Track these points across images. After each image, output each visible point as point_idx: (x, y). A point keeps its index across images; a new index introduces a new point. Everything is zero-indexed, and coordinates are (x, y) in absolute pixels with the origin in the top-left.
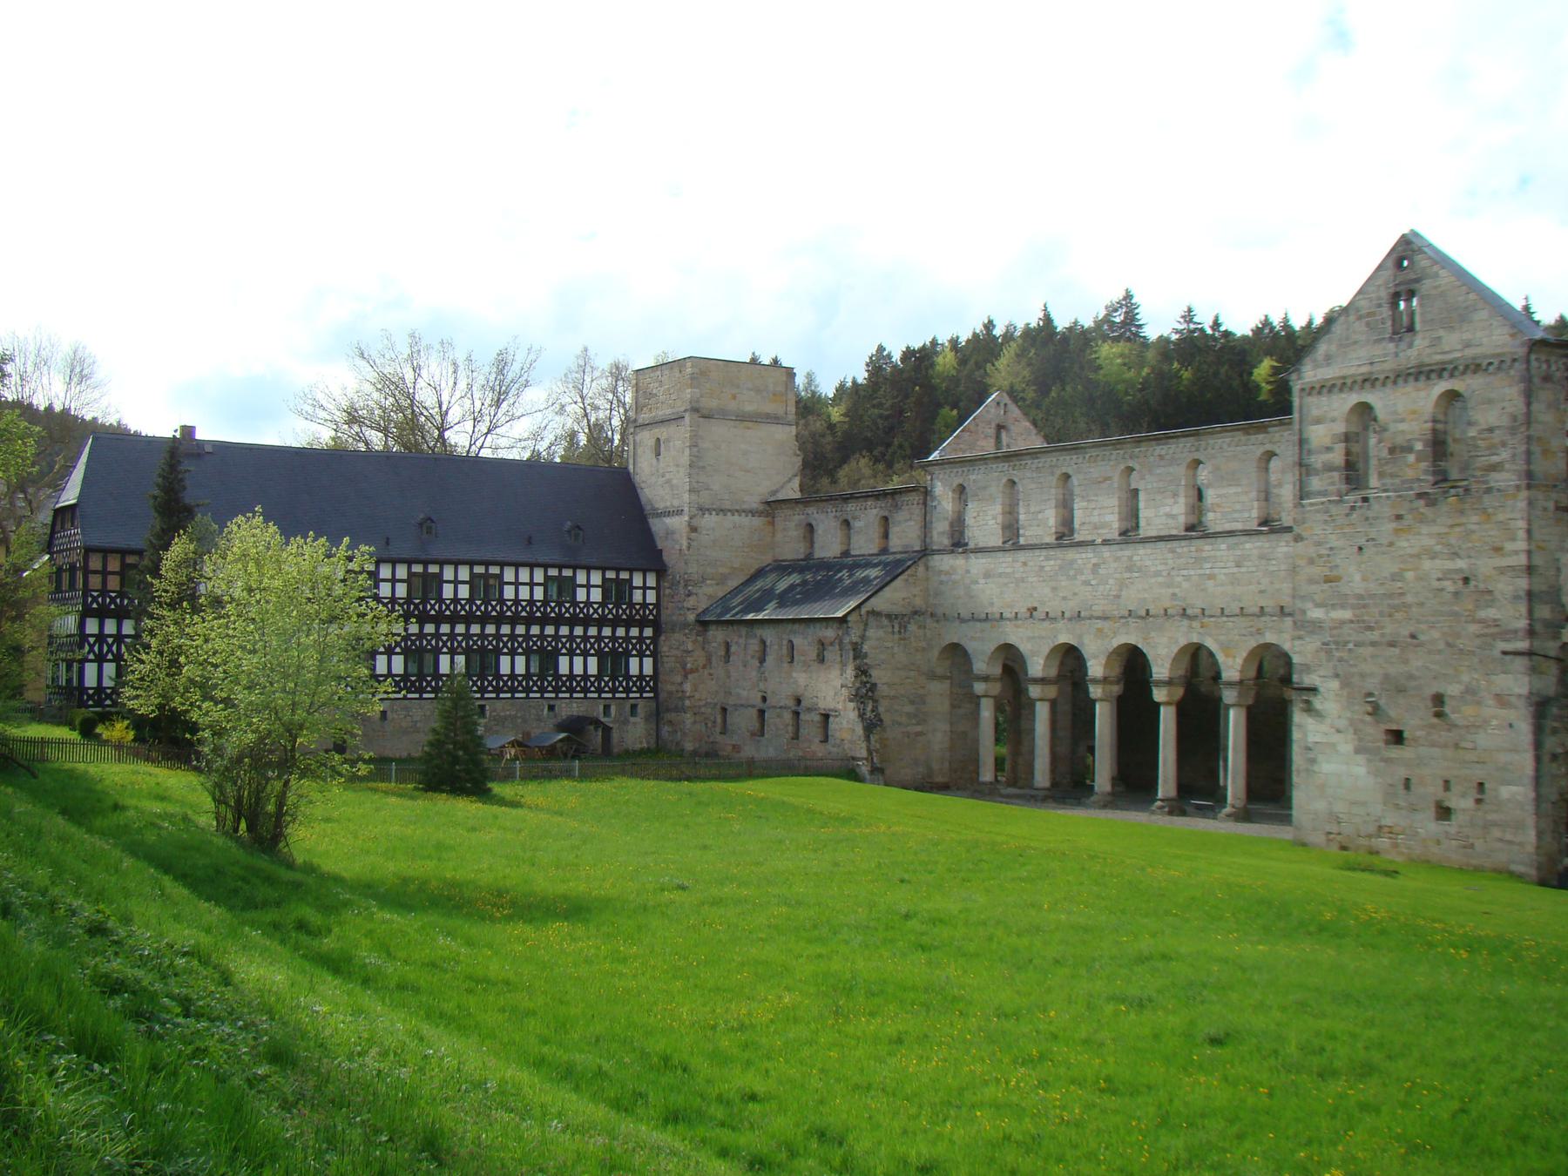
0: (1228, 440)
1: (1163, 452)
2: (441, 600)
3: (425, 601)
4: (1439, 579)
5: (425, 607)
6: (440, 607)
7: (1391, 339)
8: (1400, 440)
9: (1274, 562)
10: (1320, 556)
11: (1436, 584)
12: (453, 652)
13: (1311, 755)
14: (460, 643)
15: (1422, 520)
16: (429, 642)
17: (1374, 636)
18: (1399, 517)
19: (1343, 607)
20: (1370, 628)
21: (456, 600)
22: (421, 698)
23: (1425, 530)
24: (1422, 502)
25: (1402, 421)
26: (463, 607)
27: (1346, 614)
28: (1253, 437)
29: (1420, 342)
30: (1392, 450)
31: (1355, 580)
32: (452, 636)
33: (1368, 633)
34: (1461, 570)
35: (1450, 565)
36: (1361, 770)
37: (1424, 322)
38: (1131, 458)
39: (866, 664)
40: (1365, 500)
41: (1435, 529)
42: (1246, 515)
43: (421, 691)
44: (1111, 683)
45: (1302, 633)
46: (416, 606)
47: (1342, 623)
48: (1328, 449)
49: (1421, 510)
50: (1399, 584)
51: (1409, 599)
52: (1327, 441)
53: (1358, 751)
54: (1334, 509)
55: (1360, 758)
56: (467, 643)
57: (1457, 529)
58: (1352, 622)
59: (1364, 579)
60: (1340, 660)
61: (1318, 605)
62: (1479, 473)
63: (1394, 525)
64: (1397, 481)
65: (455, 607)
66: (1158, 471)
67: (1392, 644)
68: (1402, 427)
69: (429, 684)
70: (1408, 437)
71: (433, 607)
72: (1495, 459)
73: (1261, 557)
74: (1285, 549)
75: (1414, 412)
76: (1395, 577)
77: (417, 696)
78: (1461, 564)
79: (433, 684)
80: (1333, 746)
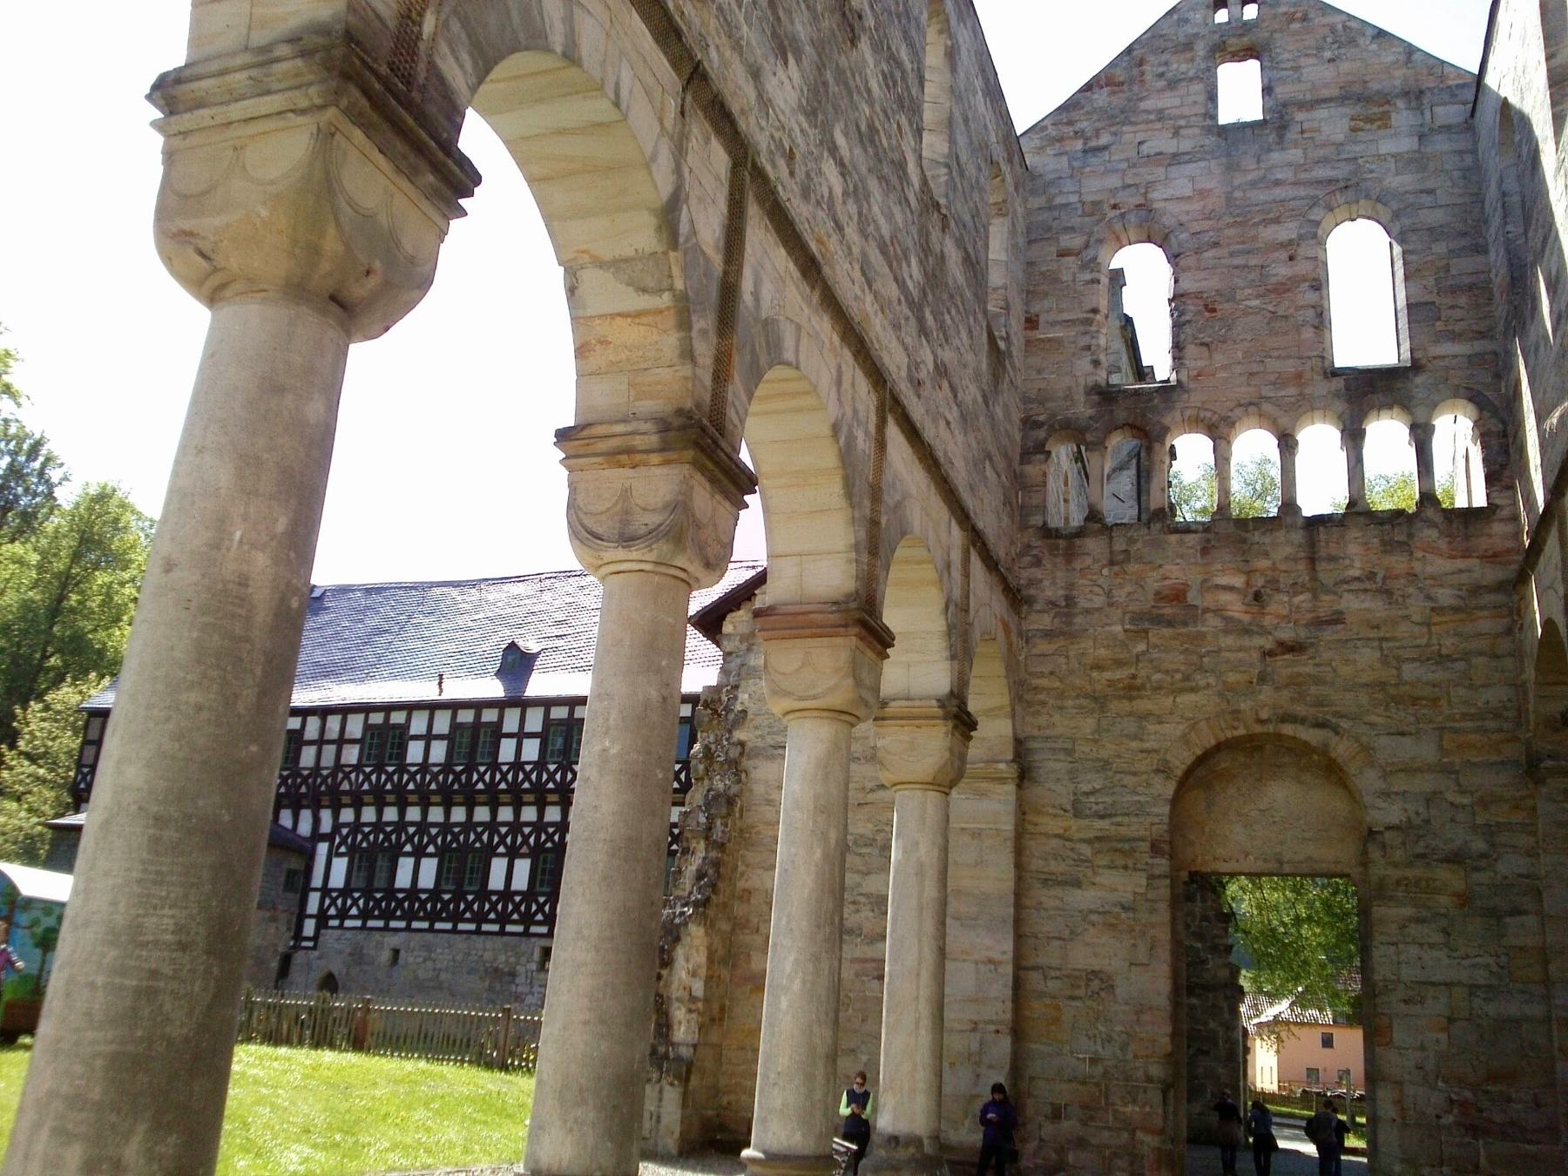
2: (495, 766)
3: (469, 770)
5: (470, 777)
6: (493, 777)
12: (513, 854)
14: (526, 838)
16: (479, 837)
21: (517, 765)
22: (454, 931)
26: (527, 777)
32: (516, 826)
39: (742, 744)
43: (456, 918)
44: (622, 455)
46: (457, 776)
56: (538, 838)
65: (515, 777)
69: (469, 906)
71: (481, 778)
77: (449, 926)
79: (476, 907)
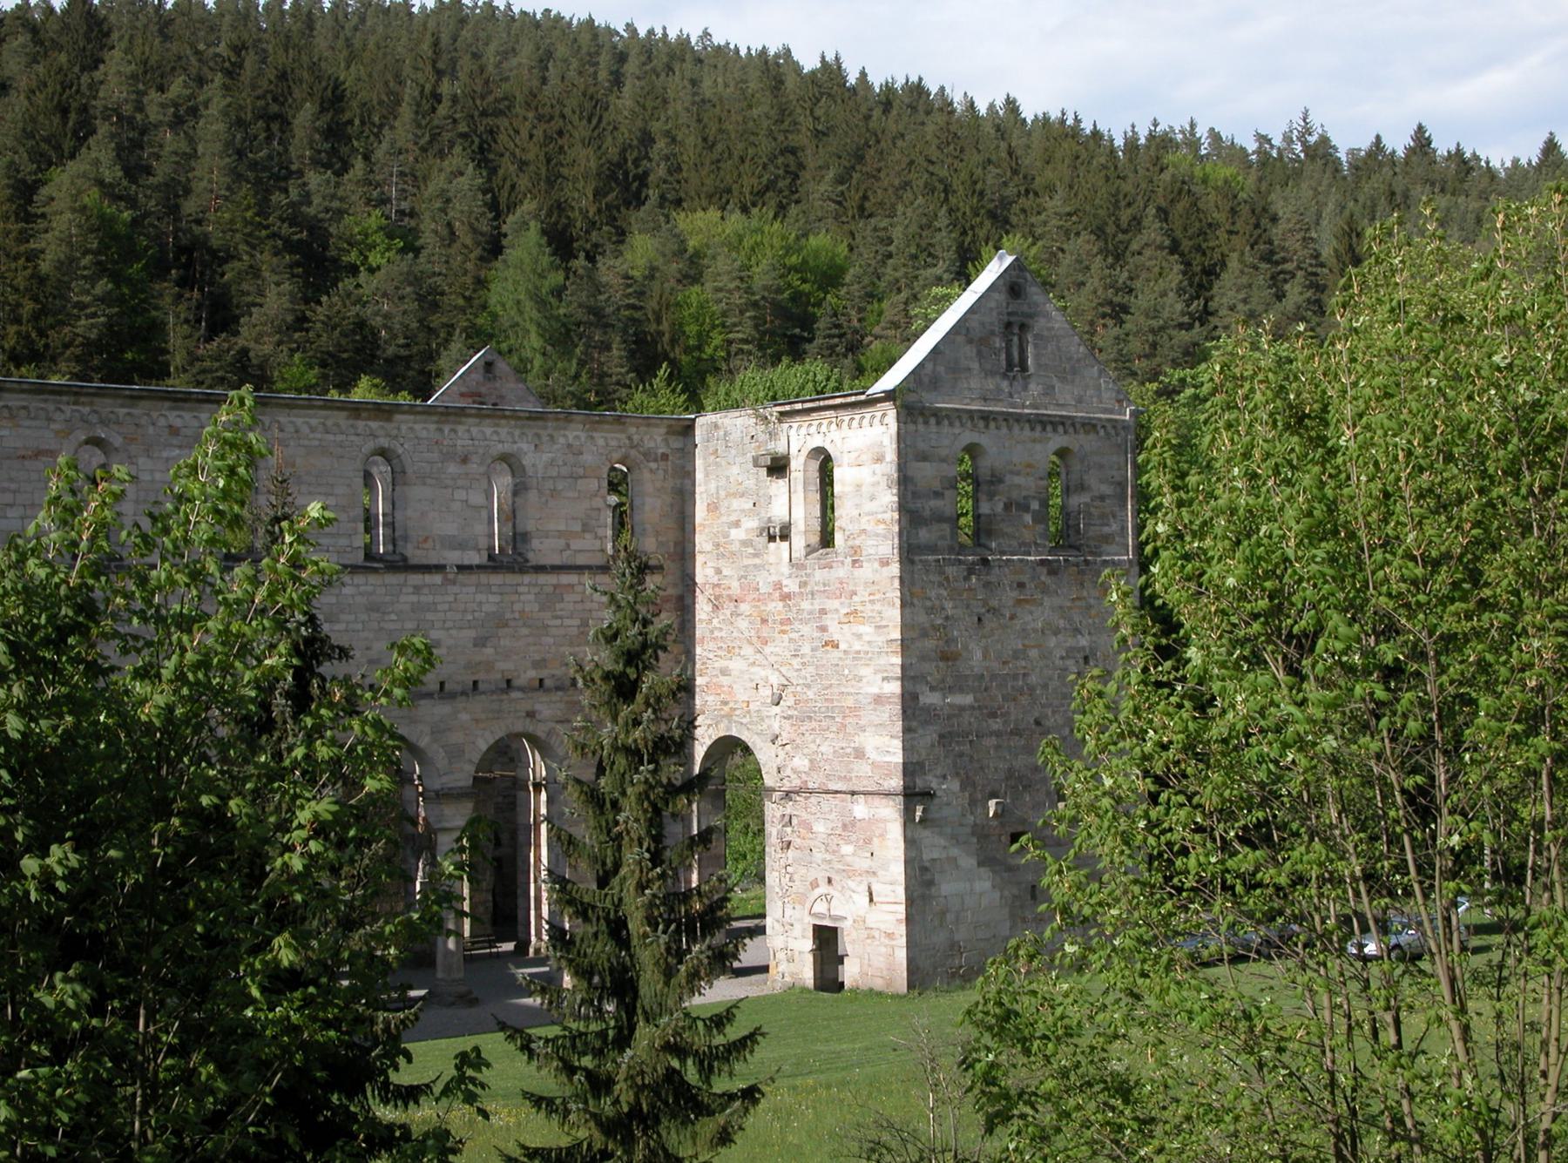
0: (314, 422)
1: (178, 423)
4: (1062, 658)
7: (1005, 376)
8: (1015, 495)
9: (393, 617)
10: (934, 627)
11: (1059, 663)
13: (928, 877)
15: (1045, 590)
17: (996, 724)
18: (1021, 585)
19: (961, 690)
20: (993, 715)
23: (1047, 602)
24: (1045, 570)
25: (1018, 473)
27: (968, 699)
28: (360, 424)
29: (1035, 389)
30: (1007, 507)
31: (976, 658)
33: (990, 721)
34: (1083, 648)
35: (1071, 642)
36: (987, 885)
37: (1039, 366)
38: (104, 422)
40: (985, 562)
41: (1057, 601)
42: (343, 542)
45: (914, 724)
47: (962, 709)
48: (938, 495)
49: (1043, 578)
50: (1023, 663)
51: (1033, 679)
52: (937, 486)
53: (980, 864)
54: (951, 571)
55: (985, 872)
57: (1078, 603)
58: (972, 708)
59: (985, 657)
60: (961, 755)
61: (932, 689)
62: (1092, 543)
63: (1015, 594)
64: (1015, 543)
66: (165, 454)
67: (1016, 732)
68: (1017, 480)
70: (1024, 493)
72: (1106, 530)
73: (373, 608)
74: (414, 598)
75: (1029, 466)
76: (1016, 655)
78: (1084, 642)
80: (953, 861)
